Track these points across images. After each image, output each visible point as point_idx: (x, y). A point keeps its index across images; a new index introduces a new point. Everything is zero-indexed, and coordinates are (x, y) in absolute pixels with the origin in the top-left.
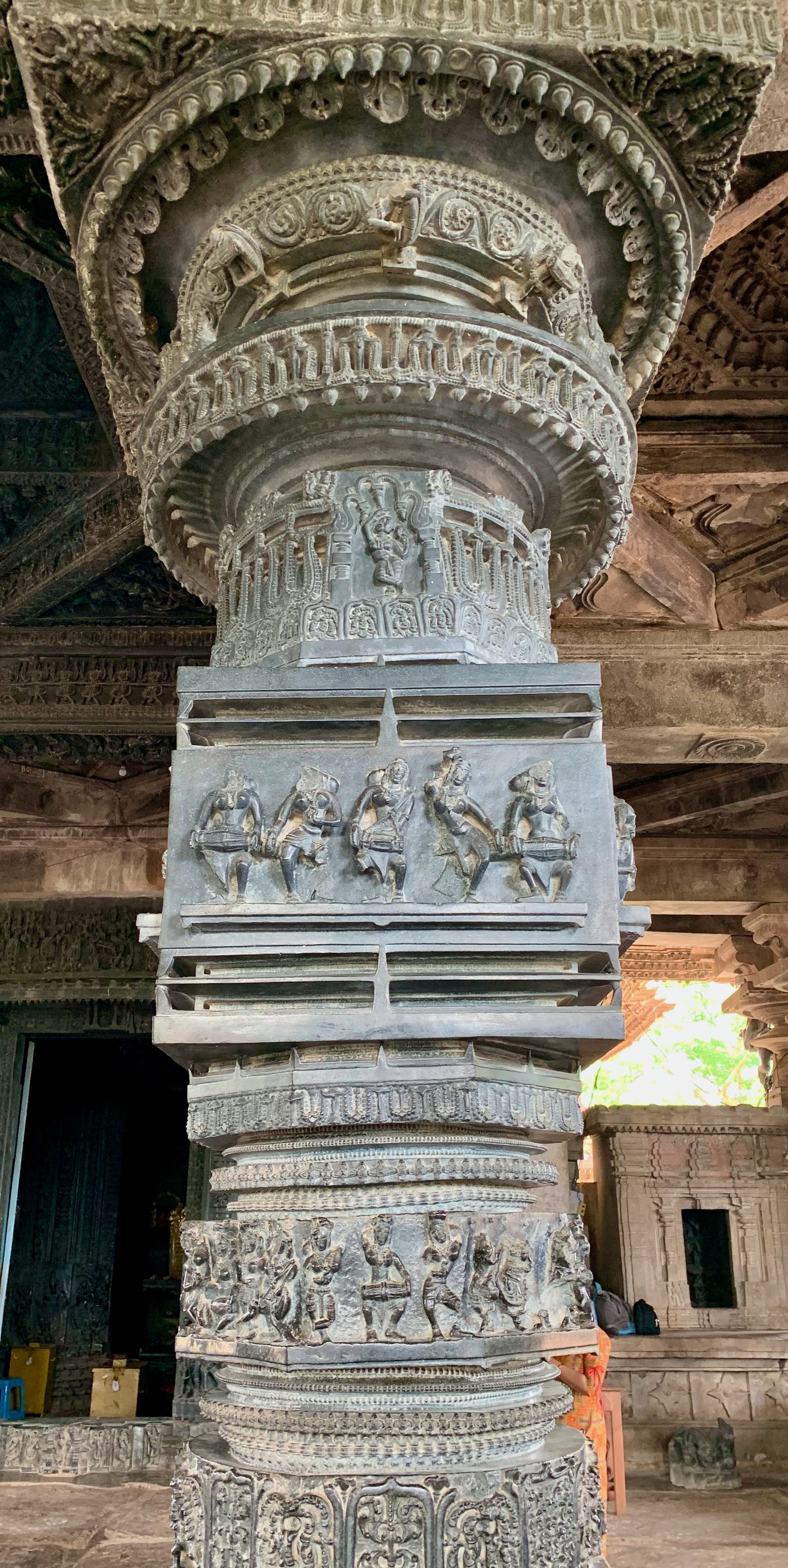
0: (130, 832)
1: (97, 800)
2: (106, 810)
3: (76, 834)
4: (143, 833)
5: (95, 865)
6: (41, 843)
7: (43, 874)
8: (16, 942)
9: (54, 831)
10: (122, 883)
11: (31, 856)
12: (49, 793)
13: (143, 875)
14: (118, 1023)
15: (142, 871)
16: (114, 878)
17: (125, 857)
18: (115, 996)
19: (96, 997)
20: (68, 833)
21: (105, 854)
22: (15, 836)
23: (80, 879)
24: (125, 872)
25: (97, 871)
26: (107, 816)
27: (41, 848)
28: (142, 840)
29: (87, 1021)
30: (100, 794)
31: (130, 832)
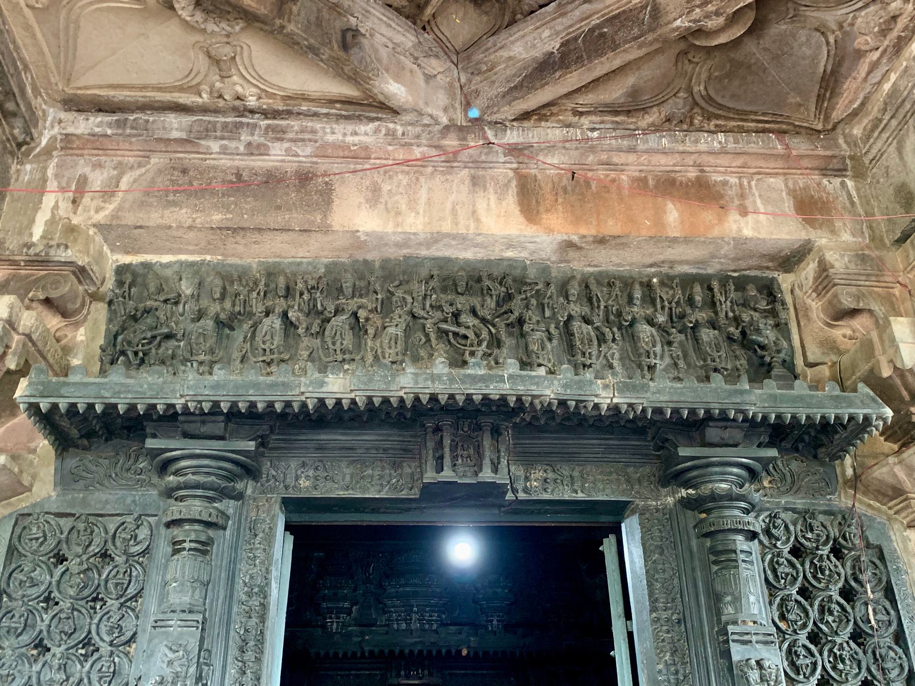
0: (490, 134)
1: (429, 78)
2: (442, 98)
3: (391, 134)
4: (513, 136)
5: (423, 194)
6: (323, 151)
7: (329, 202)
8: (278, 323)
9: (350, 127)
10: (478, 220)
11: (304, 178)
12: (356, 33)
13: (515, 209)
14: (495, 470)
15: (511, 200)
16: (462, 214)
17: (476, 182)
18: (521, 389)
19: (477, 392)
20: (377, 131)
21: (439, 178)
22: (279, 134)
23: (398, 213)
24: (481, 205)
25: (429, 202)
26: (445, 110)
27: (323, 165)
28: (514, 150)
29: (430, 464)
30: (436, 65)
31: (490, 134)
